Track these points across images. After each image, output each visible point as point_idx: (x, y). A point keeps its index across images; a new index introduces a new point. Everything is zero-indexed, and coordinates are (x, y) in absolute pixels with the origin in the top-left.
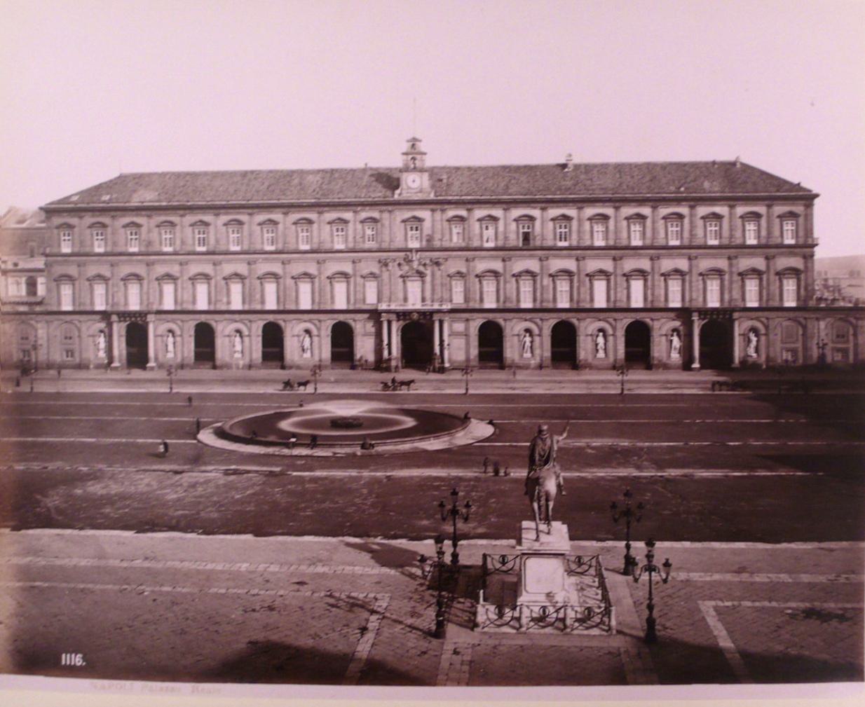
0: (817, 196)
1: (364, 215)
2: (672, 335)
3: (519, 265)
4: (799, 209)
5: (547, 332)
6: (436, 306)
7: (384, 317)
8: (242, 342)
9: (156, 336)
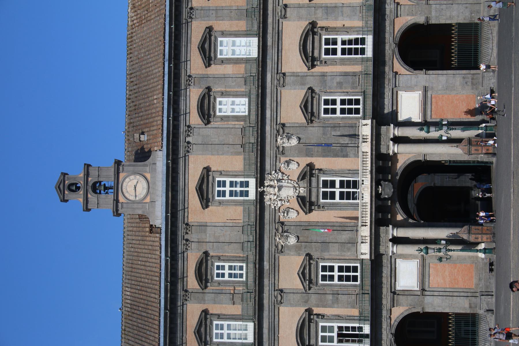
1: (192, 282)
6: (366, 147)
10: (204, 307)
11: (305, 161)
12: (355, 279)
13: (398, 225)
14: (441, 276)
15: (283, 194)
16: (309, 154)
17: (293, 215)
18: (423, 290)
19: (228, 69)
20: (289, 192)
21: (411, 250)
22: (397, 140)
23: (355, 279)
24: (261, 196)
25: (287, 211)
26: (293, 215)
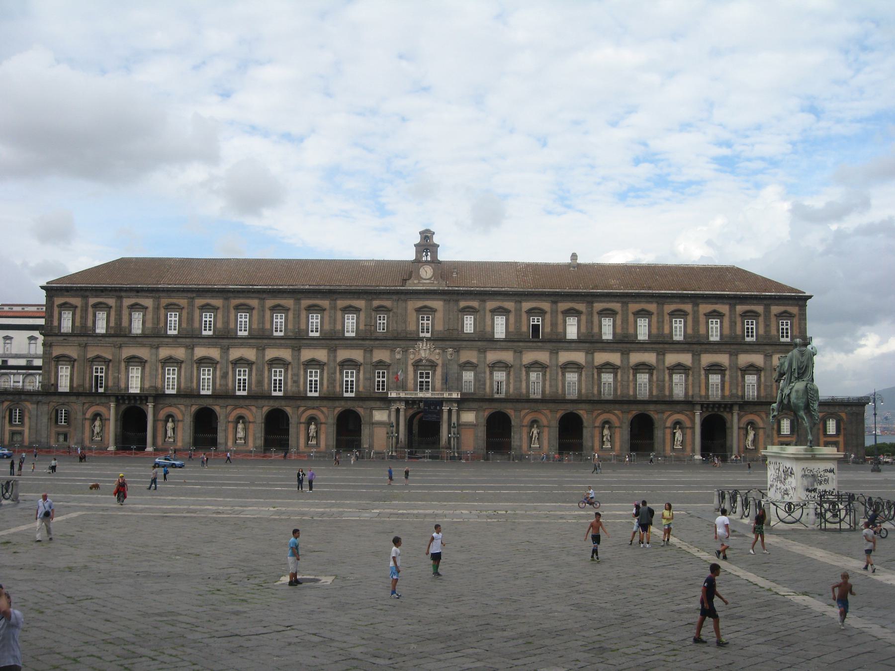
0: (810, 297)
1: (376, 303)
2: (675, 428)
3: (529, 357)
4: (794, 310)
5: (555, 424)
6: (446, 395)
8: (245, 429)
9: (155, 421)
10: (363, 310)
11: (440, 362)
12: (378, 389)
13: (405, 410)
14: (380, 434)
15: (424, 351)
16: (443, 365)
17: (412, 356)
18: (373, 424)
19: (488, 322)
20: (423, 354)
21: (393, 419)
22: (450, 411)
23: (378, 389)
24: (421, 339)
25: (414, 354)
26: (412, 356)
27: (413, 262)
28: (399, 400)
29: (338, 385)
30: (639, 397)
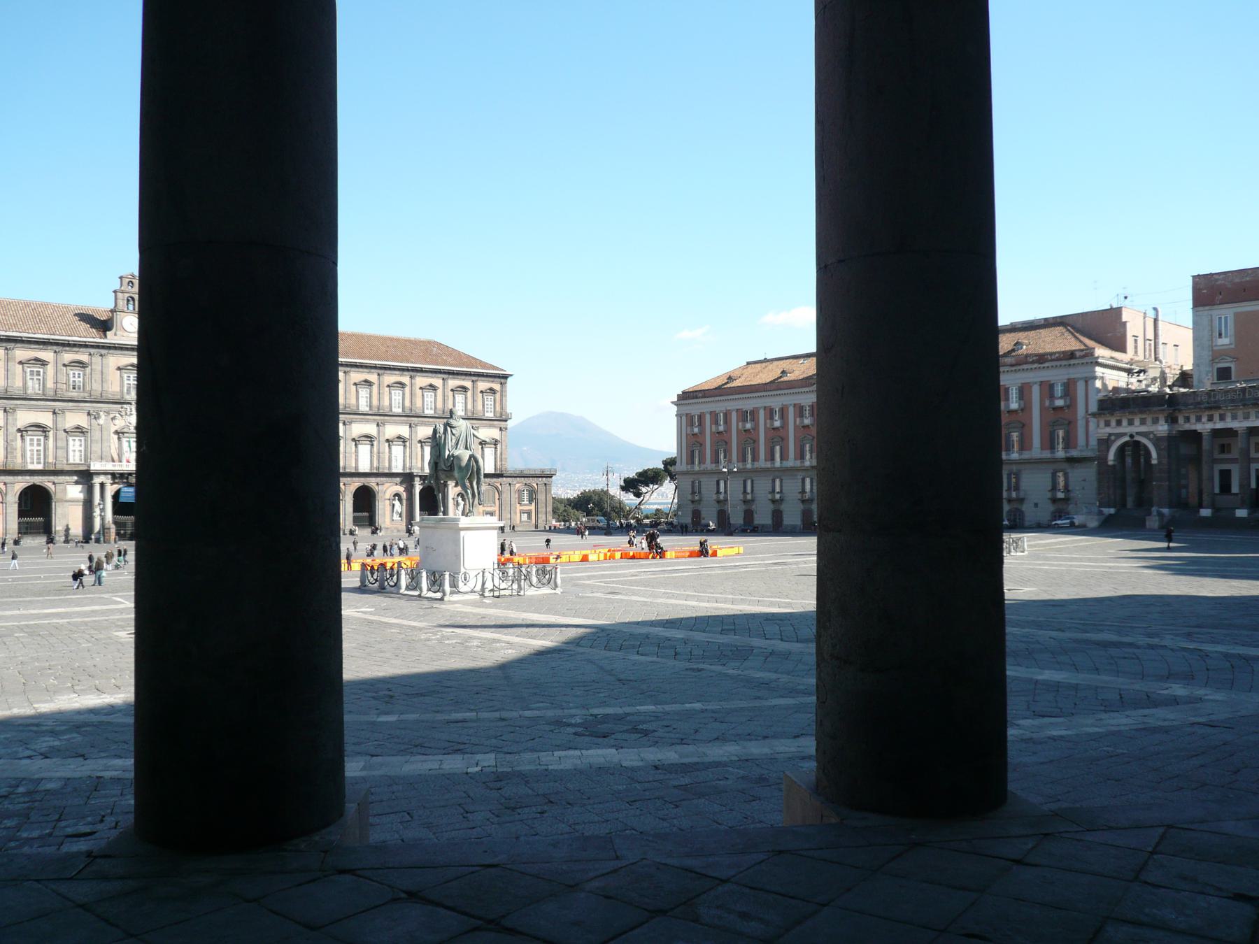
4: (497, 387)
7: (97, 481)
27: (112, 311)
28: (105, 473)
29: (19, 455)
30: (361, 470)
